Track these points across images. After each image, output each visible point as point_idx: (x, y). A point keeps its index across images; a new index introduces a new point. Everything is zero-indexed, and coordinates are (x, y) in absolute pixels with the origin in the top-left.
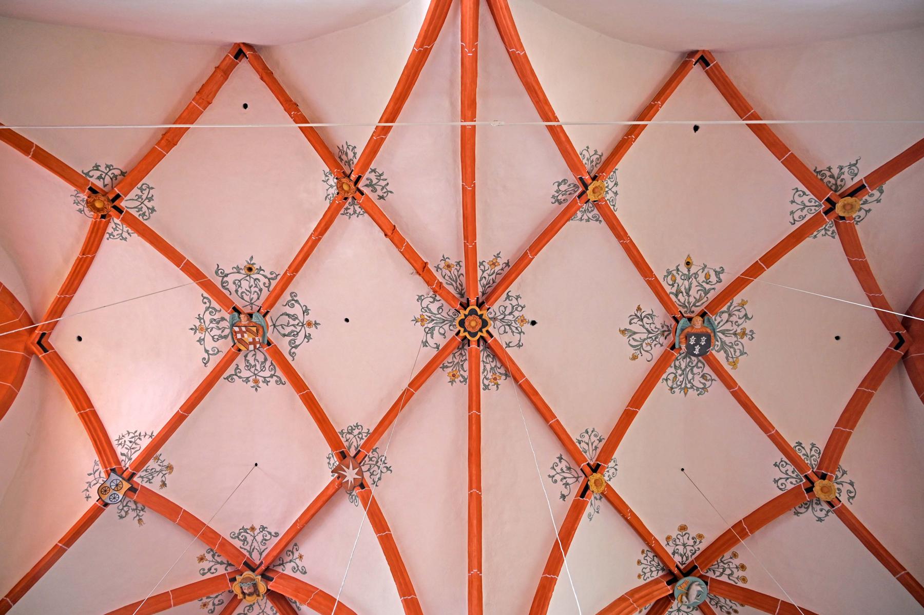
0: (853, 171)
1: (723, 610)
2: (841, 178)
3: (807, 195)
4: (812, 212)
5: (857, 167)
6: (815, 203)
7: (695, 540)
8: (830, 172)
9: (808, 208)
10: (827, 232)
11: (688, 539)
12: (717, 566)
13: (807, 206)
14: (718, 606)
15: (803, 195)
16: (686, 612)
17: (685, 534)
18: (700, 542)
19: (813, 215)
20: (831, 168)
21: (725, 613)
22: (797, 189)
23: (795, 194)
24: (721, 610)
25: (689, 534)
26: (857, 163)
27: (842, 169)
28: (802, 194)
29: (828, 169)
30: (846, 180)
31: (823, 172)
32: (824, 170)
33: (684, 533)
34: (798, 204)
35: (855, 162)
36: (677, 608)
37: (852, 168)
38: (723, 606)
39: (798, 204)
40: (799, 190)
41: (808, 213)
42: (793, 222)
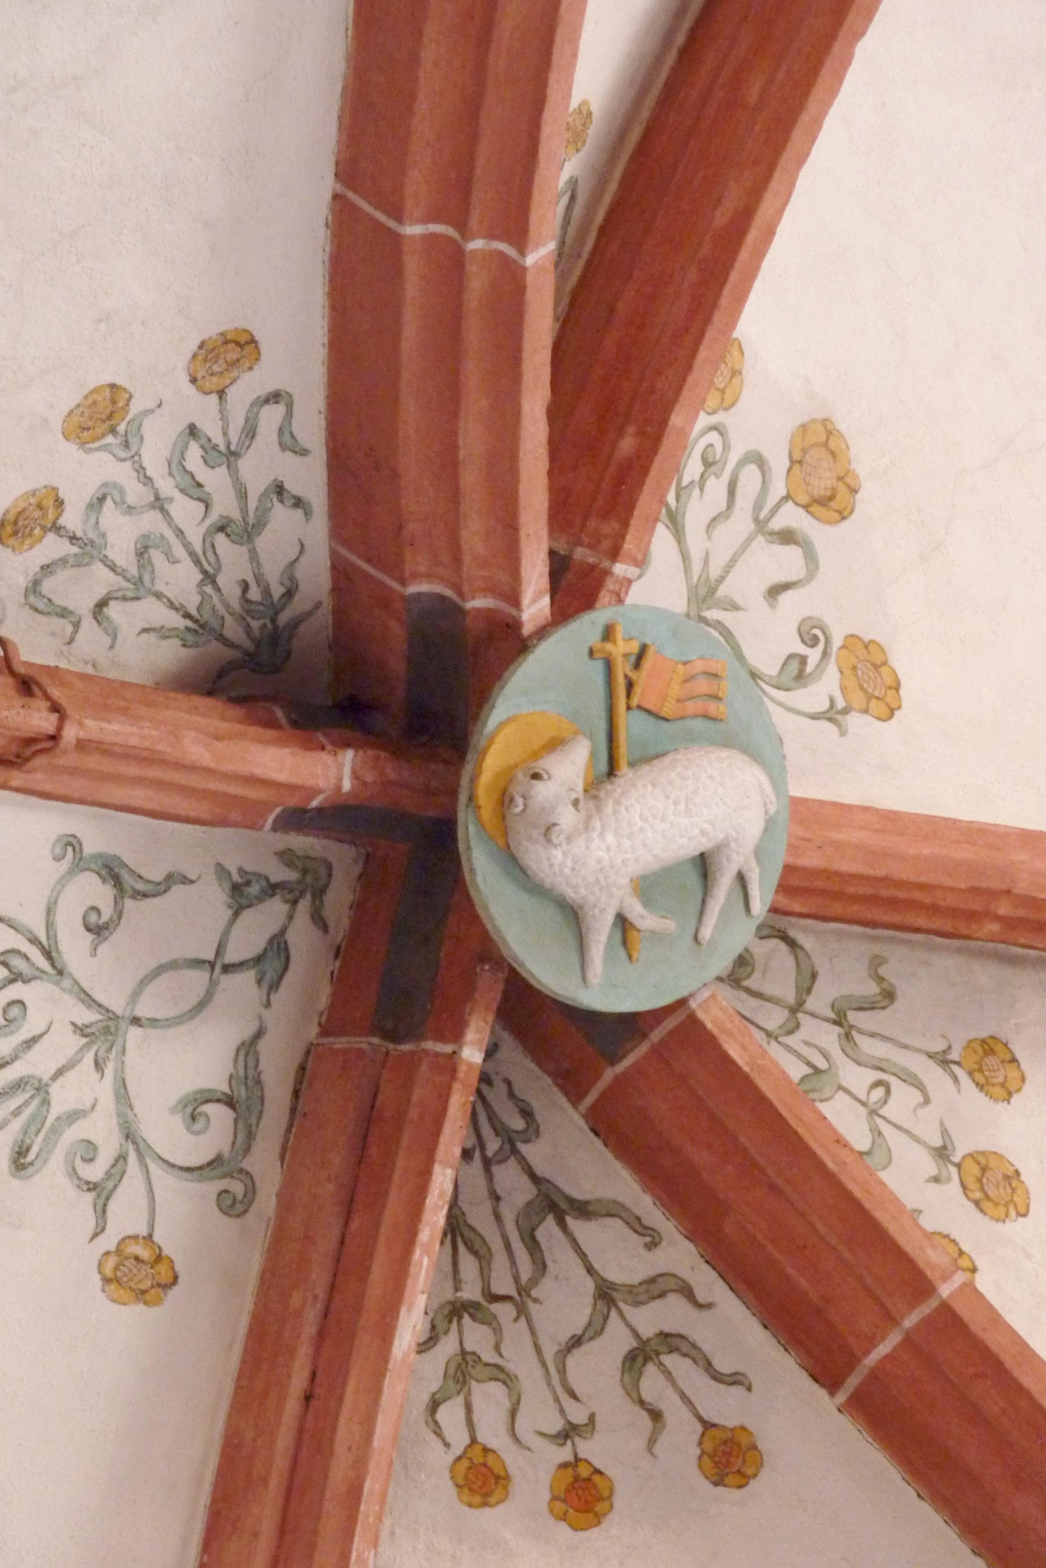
1: (450, 1415)
7: (814, 655)
11: (775, 591)
12: (774, 1018)
14: (448, 1346)
16: (130, 1135)
17: (787, 537)
18: (832, 715)
21: (440, 1459)
24: (434, 1405)
25: (811, 558)
33: (791, 517)
36: (116, 1002)
38: (502, 1375)
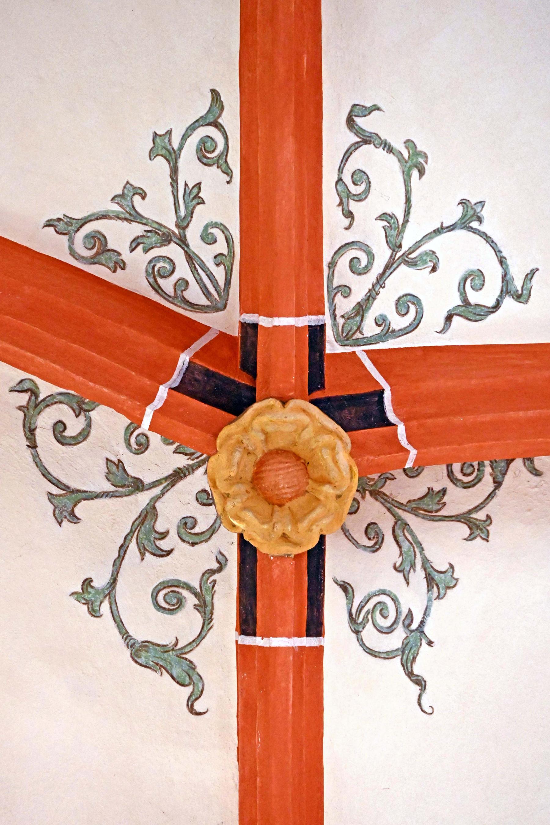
0: (385, 623)
2: (389, 539)
3: (449, 318)
4: (344, 262)
5: (388, 655)
6: (382, 321)
8: (457, 518)
9: (378, 267)
10: (137, 229)
13: (389, 267)
15: (466, 302)
19: (327, 257)
20: (470, 538)
22: (518, 297)
23: (502, 261)
26: (410, 674)
27: (430, 580)
28: (474, 297)
29: (481, 515)
30: (367, 555)
31: (487, 483)
32: (491, 496)
34: (438, 232)
35: (417, 670)
37: (399, 635)
39: (438, 232)
40: (508, 302)
41: (349, 237)
42: (360, 121)
